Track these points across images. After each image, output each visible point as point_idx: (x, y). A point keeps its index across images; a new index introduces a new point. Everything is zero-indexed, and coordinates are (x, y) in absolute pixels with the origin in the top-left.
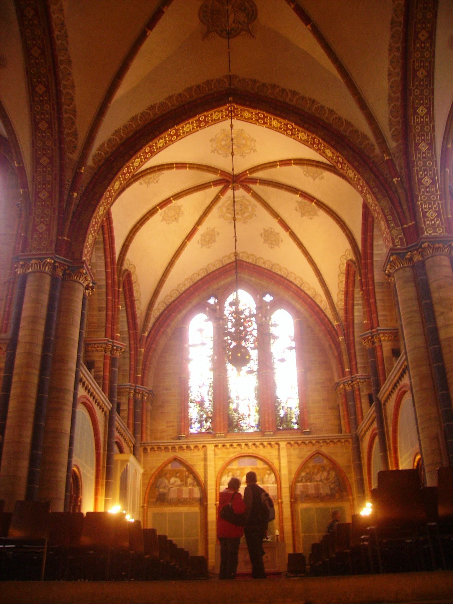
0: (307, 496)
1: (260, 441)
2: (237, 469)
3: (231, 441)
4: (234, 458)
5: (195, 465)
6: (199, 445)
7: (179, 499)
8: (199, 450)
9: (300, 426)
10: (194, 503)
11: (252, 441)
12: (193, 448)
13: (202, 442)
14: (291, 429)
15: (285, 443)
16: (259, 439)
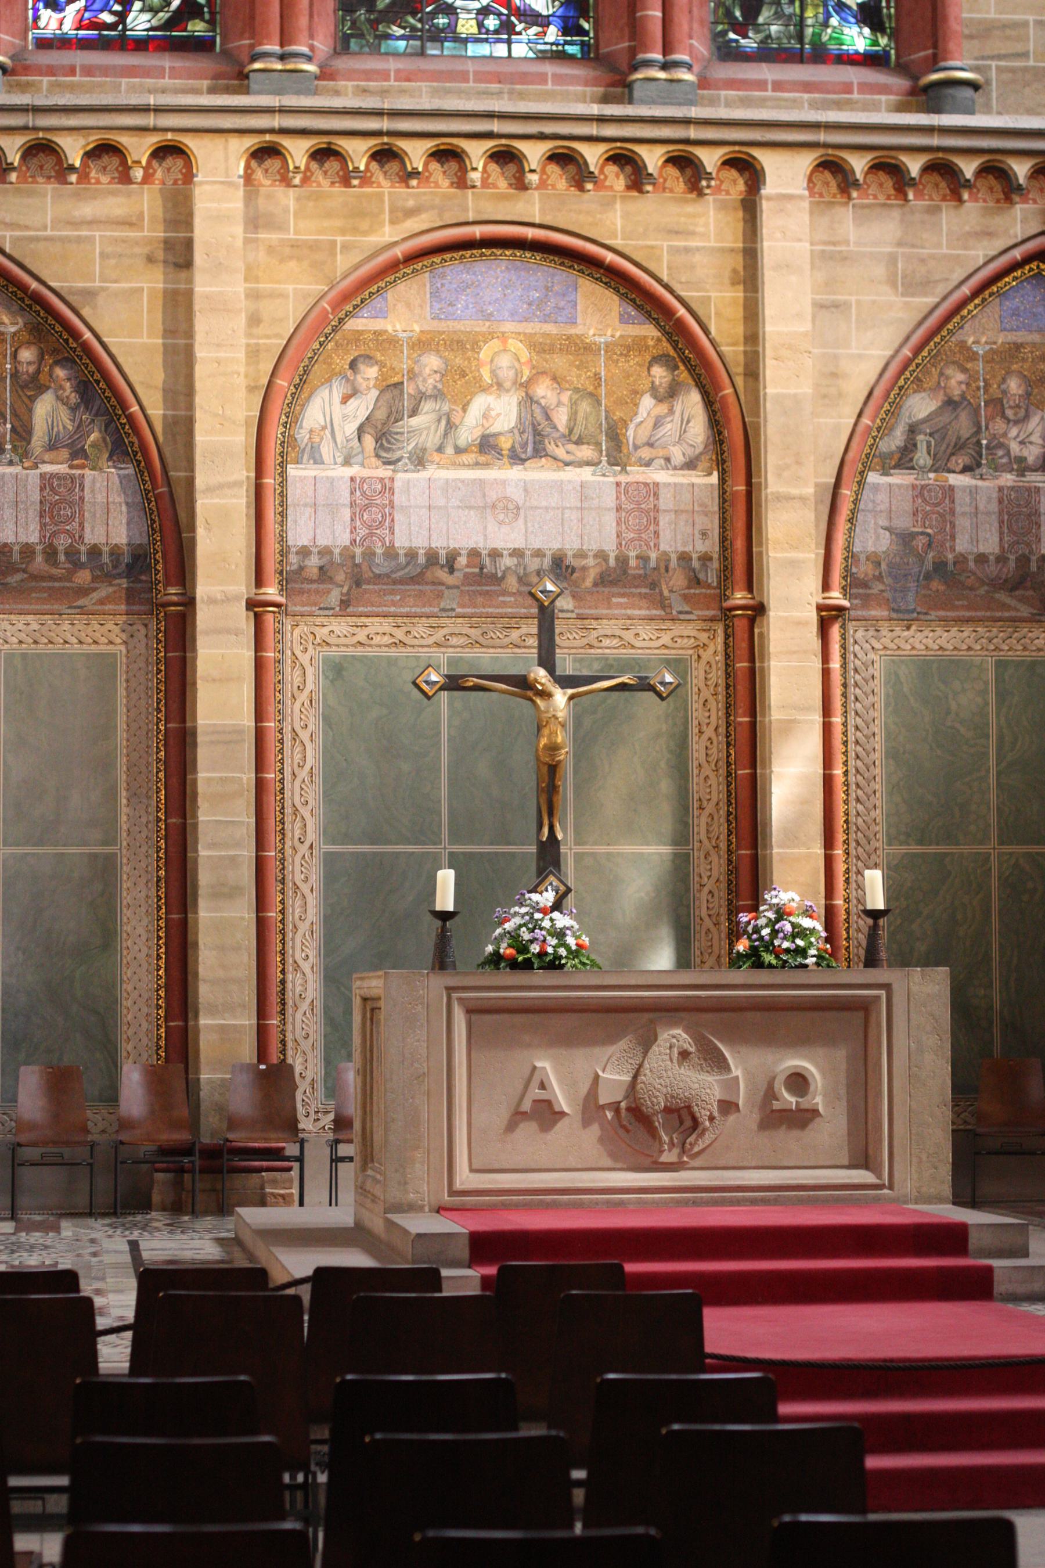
0: (940, 566)
1: (609, 131)
2: (423, 344)
3: (385, 124)
4: (398, 252)
5: (90, 294)
6: (125, 140)
8: (125, 178)
9: (894, 35)
11: (549, 128)
12: (77, 164)
13: (150, 120)
14: (820, 55)
15: (806, 161)
16: (601, 120)
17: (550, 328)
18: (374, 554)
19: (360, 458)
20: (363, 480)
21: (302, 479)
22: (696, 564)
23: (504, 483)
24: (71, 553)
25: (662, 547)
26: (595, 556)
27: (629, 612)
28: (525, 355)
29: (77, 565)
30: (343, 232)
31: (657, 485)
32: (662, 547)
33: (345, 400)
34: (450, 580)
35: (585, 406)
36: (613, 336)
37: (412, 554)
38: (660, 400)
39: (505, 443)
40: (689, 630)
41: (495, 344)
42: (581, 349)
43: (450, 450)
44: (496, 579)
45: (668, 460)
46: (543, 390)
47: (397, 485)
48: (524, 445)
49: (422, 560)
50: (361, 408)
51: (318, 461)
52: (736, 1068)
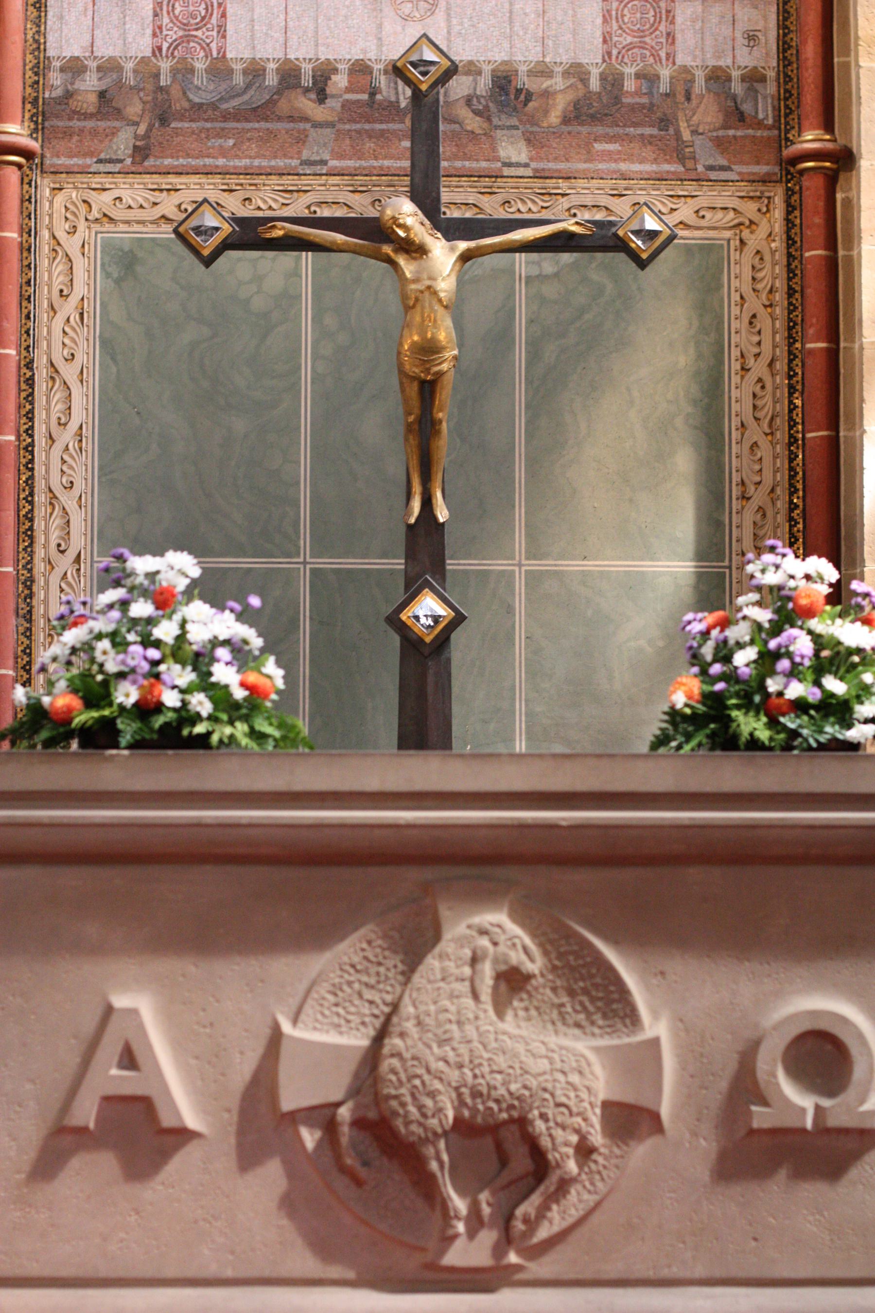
18: (192, 71)
22: (737, 88)
25: (682, 59)
26: (566, 74)
27: (623, 166)
32: (682, 59)
34: (318, 112)
37: (255, 71)
40: (726, 197)
49: (271, 80)
52: (656, 1015)
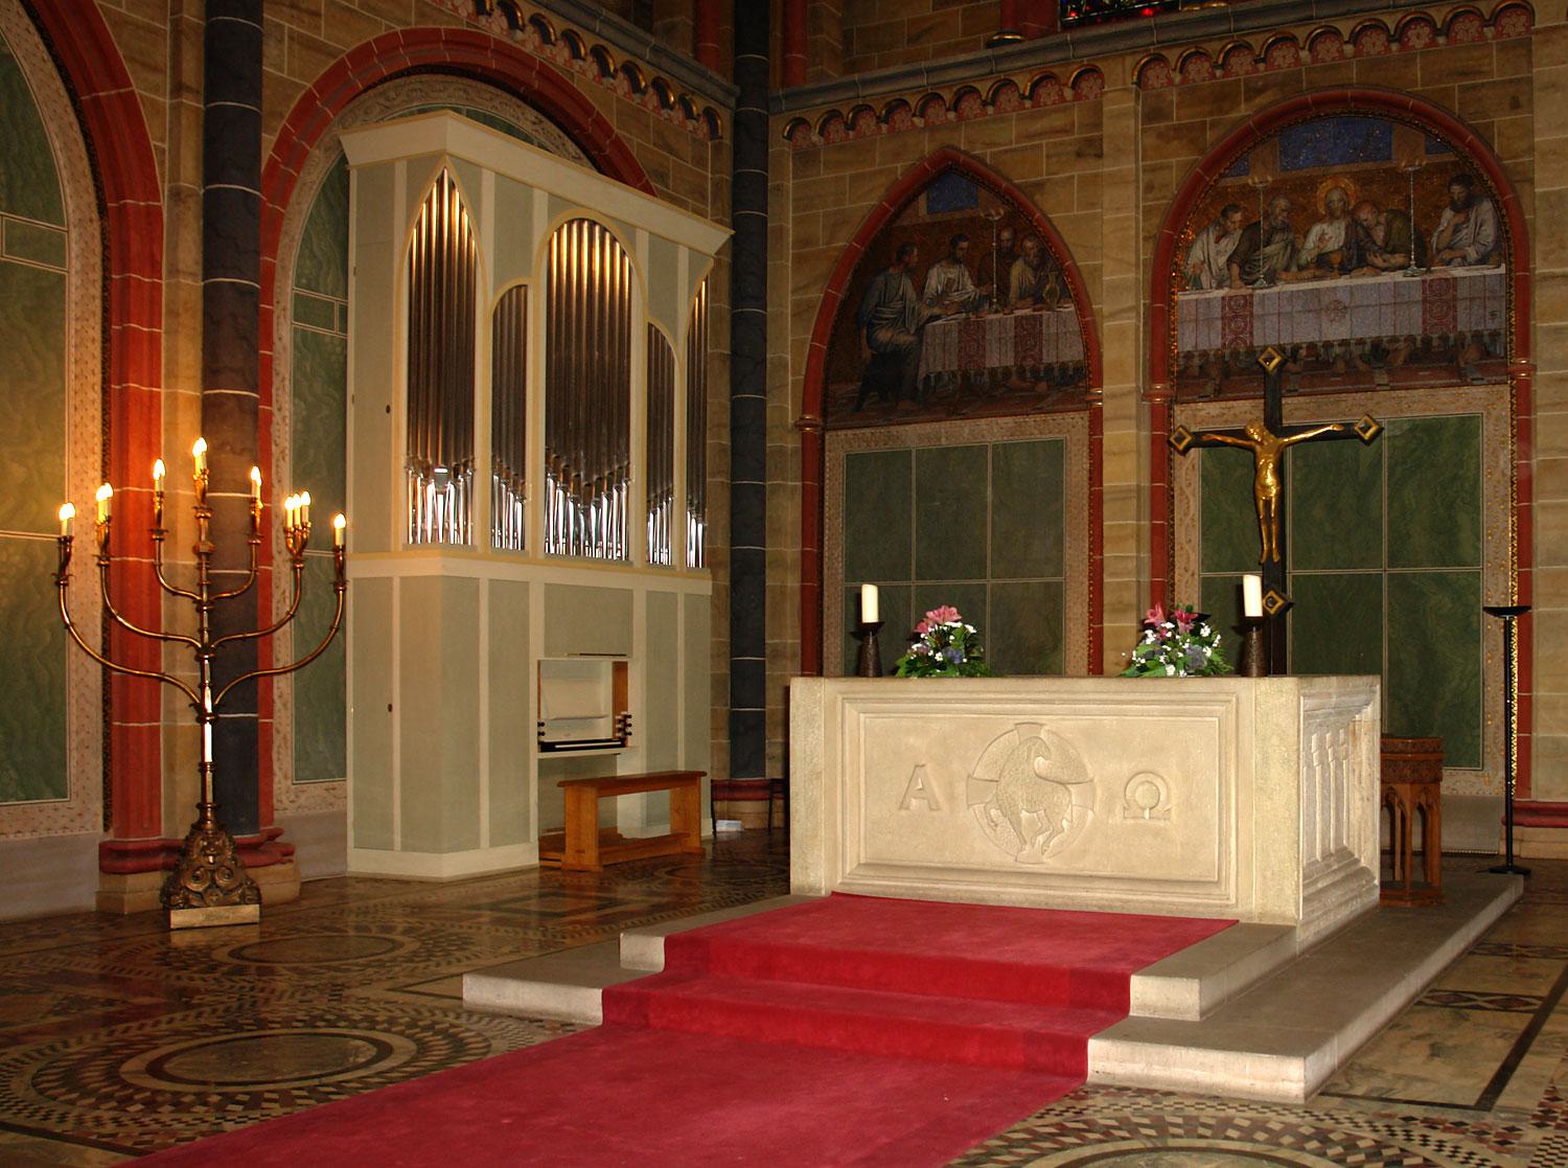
2: (1273, 192)
7: (965, 376)
10: (1042, 397)
17: (1370, 165)
18: (1239, 353)
19: (1228, 282)
20: (1231, 298)
21: (1188, 302)
22: (1486, 339)
23: (1335, 289)
24: (1035, 371)
25: (1460, 328)
26: (1406, 340)
27: (1432, 382)
28: (1352, 188)
29: (1038, 379)
30: (1211, 113)
31: (1455, 279)
32: (1460, 328)
33: (1217, 241)
35: (1398, 224)
36: (1420, 165)
38: (1457, 210)
39: (1336, 259)
41: (1329, 184)
42: (1396, 178)
43: (1294, 269)
44: (1328, 365)
45: (1464, 258)
46: (1365, 215)
47: (1256, 299)
48: (1350, 260)
50: (1229, 245)
51: (1198, 286)
